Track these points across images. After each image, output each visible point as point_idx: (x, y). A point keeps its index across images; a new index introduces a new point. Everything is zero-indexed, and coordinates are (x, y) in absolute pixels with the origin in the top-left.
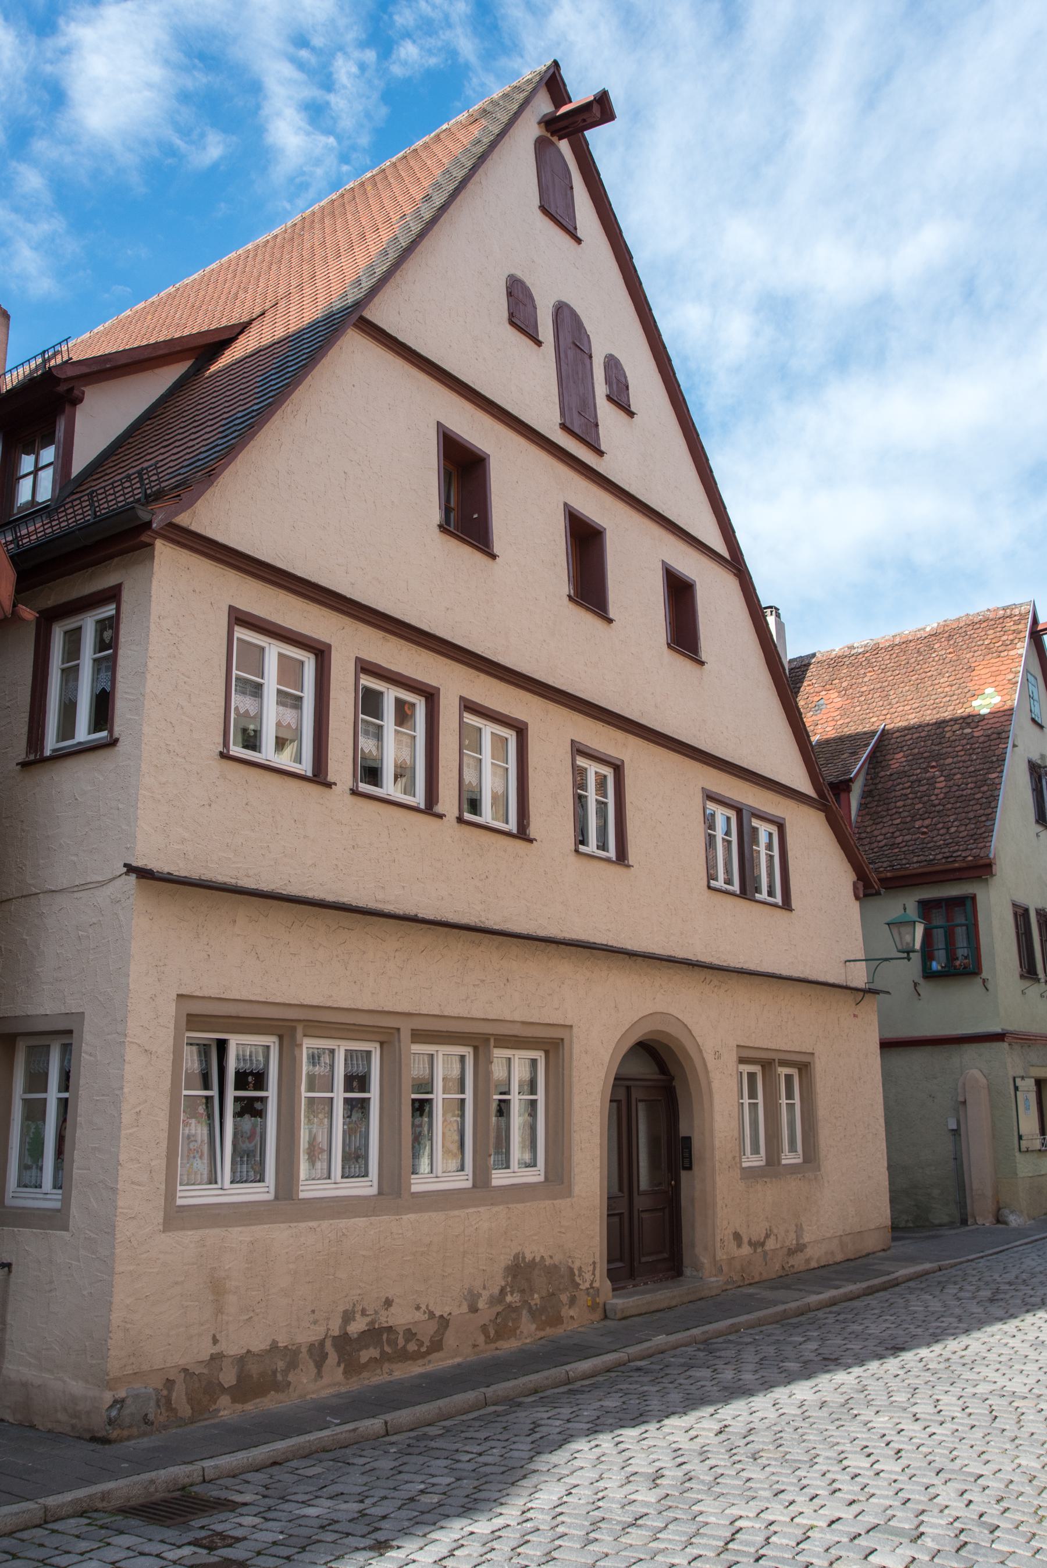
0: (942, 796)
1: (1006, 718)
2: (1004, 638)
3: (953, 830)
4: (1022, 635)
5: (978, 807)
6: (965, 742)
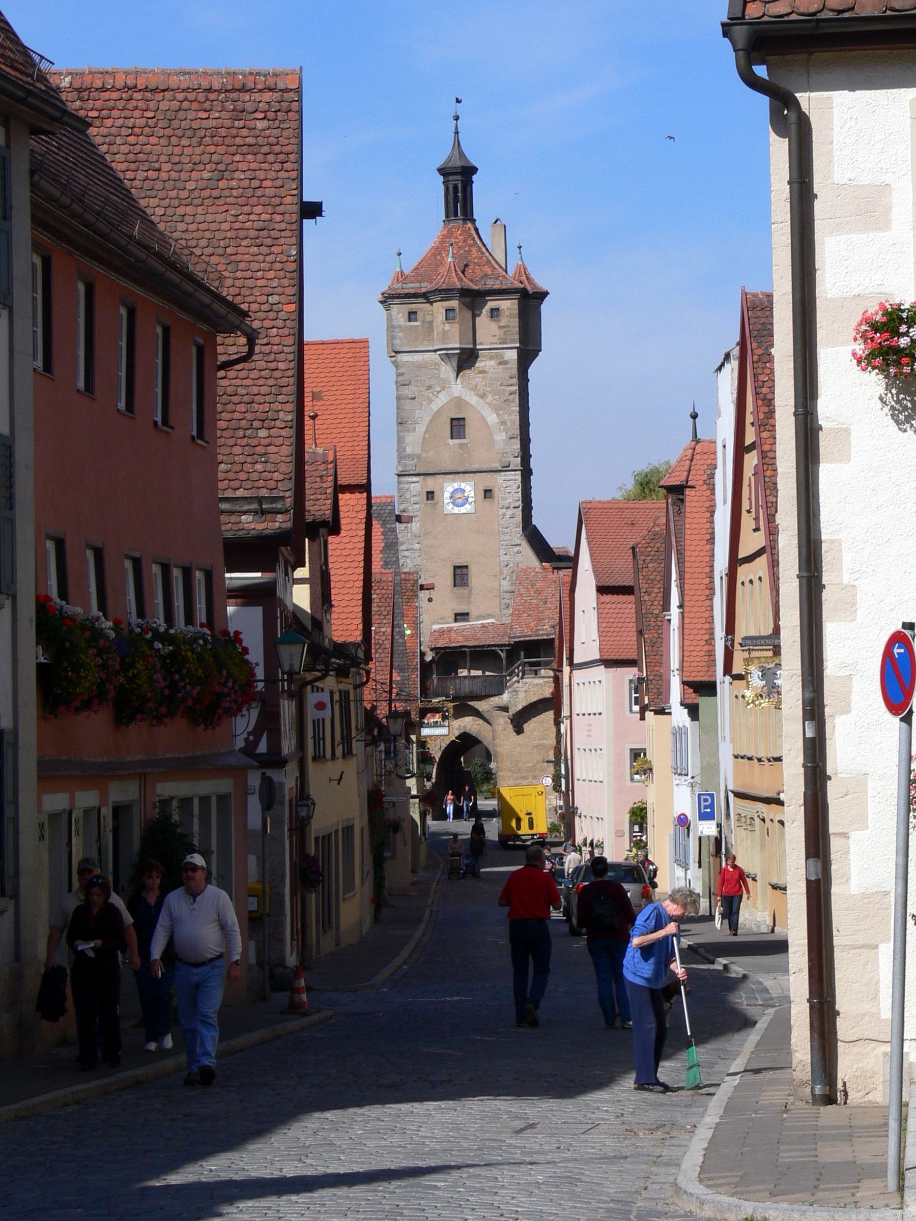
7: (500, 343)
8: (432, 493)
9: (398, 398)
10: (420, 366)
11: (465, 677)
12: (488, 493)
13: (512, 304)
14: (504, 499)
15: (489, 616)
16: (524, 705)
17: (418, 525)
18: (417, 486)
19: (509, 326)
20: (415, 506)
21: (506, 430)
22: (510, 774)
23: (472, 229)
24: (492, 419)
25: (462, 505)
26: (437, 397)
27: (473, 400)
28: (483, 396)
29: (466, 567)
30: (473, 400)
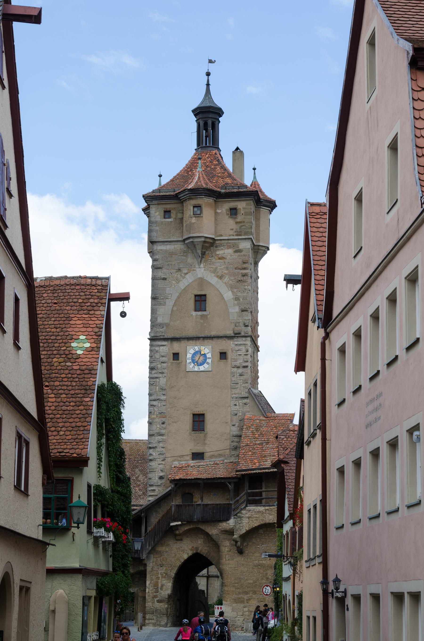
0: (53, 408)
1: (95, 360)
2: (92, 300)
3: (62, 433)
4: (103, 301)
5: (78, 420)
6: (67, 372)
7: (237, 235)
8: (178, 354)
9: (153, 279)
10: (172, 254)
11: (199, 505)
12: (223, 355)
13: (247, 205)
14: (236, 360)
15: (220, 455)
16: (247, 529)
17: (165, 380)
18: (166, 349)
19: (244, 222)
20: (163, 364)
21: (238, 304)
22: (234, 589)
23: (218, 154)
24: (228, 295)
25: (201, 364)
26: (184, 278)
27: (213, 280)
28: (221, 277)
29: (203, 415)
30: (213, 280)
